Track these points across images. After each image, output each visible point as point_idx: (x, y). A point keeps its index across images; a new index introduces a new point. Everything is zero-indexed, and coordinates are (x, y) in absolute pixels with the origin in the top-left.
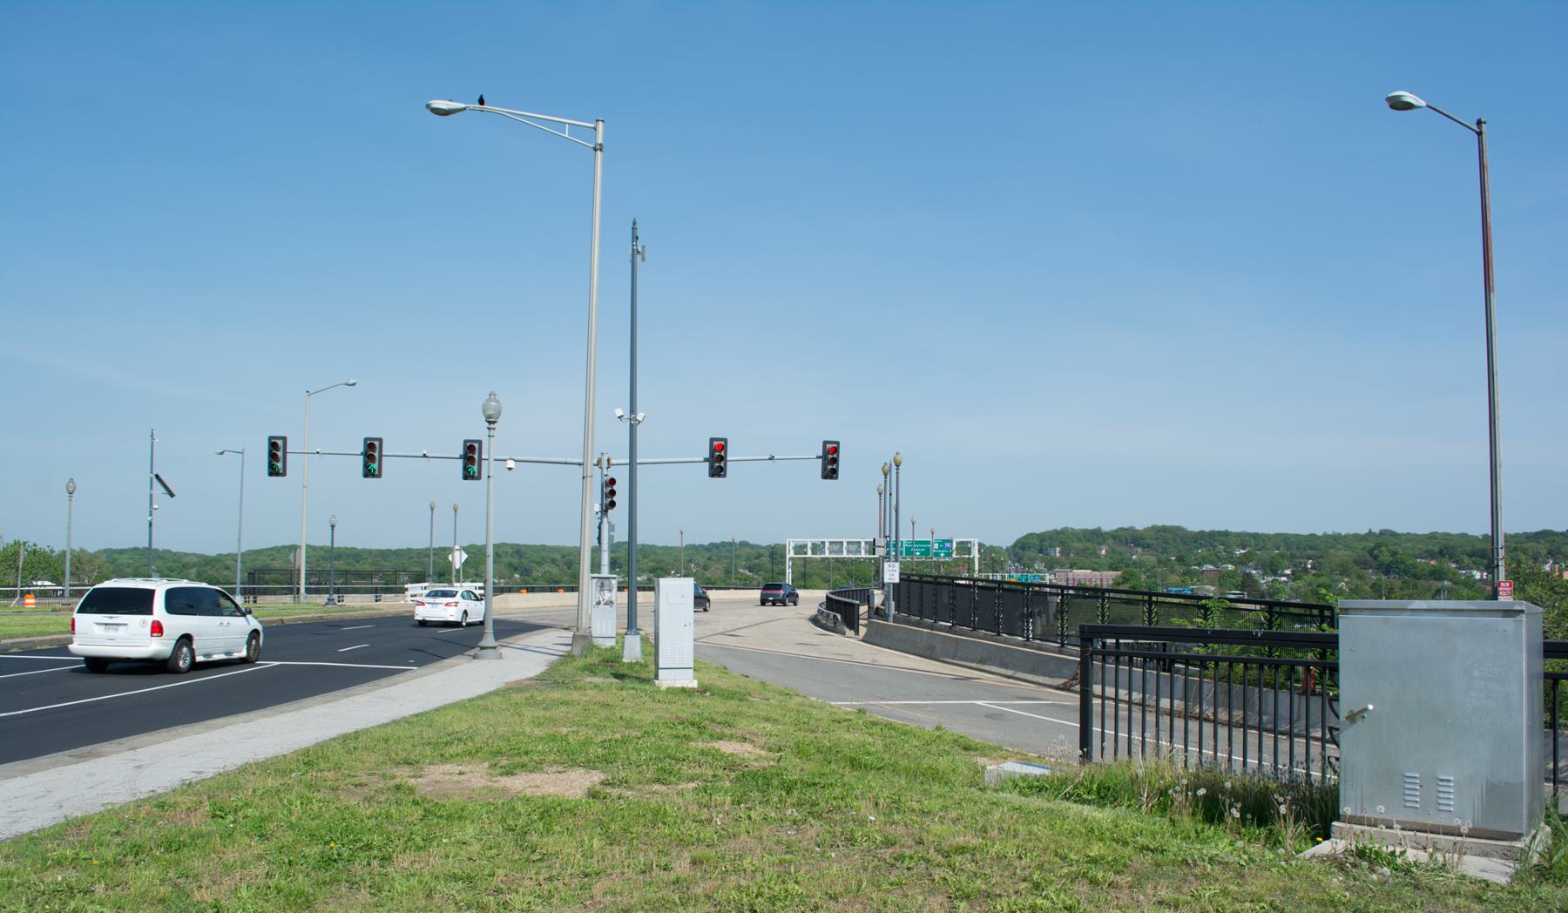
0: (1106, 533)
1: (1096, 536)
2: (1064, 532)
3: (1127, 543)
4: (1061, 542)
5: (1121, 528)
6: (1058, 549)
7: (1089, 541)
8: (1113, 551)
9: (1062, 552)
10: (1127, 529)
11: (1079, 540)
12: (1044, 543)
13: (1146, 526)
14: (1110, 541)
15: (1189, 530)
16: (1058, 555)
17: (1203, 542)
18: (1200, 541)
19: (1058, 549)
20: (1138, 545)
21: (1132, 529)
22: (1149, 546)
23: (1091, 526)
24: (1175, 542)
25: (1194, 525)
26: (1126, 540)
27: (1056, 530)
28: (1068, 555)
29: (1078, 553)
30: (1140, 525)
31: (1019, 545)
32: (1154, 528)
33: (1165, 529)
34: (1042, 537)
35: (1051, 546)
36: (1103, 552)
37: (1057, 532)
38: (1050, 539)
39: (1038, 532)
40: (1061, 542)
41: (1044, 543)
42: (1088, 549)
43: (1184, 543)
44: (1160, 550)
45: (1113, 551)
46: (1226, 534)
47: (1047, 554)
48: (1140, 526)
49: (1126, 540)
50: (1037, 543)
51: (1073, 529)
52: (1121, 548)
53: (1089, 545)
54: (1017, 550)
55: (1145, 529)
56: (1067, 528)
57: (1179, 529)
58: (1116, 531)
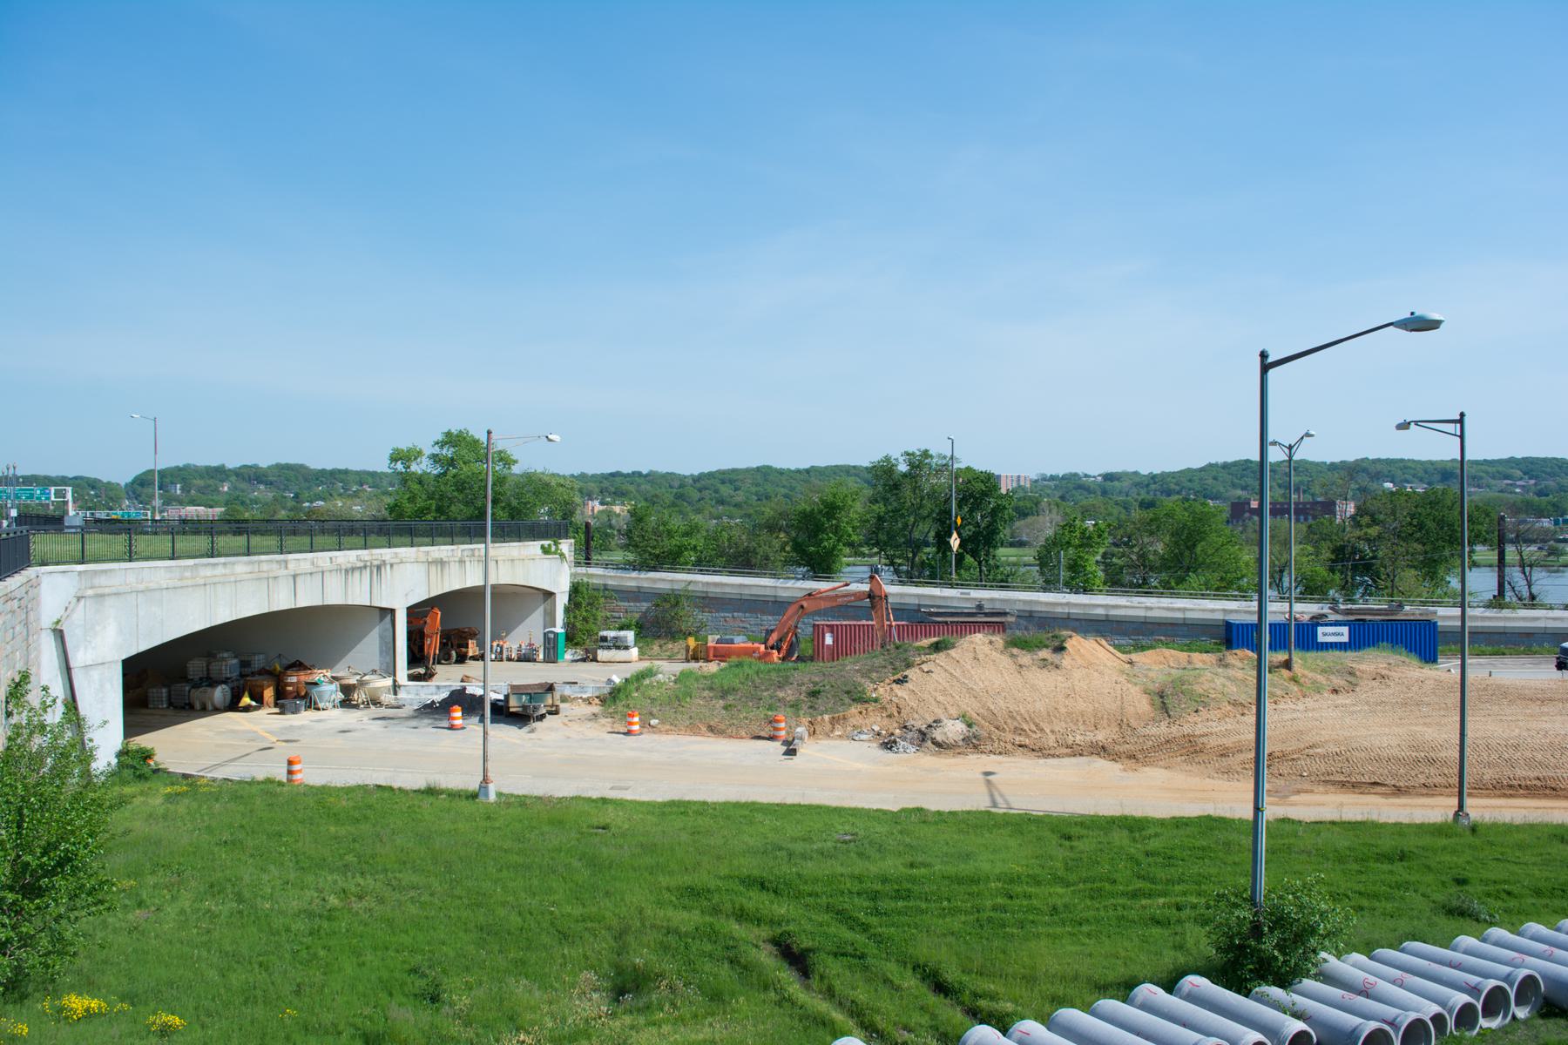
0: (230, 470)
1: (219, 473)
2: (186, 468)
3: (250, 480)
4: (183, 479)
6: (178, 486)
7: (212, 477)
8: (235, 488)
9: (182, 489)
10: (251, 467)
11: (202, 477)
12: (165, 480)
13: (270, 464)
14: (233, 478)
15: (312, 467)
16: (178, 492)
19: (178, 486)
20: (260, 482)
21: (255, 467)
22: (271, 483)
23: (214, 464)
26: (250, 477)
27: (177, 467)
28: (189, 491)
29: (201, 490)
33: (289, 467)
35: (172, 483)
36: (226, 489)
37: (178, 469)
38: (172, 476)
40: (183, 479)
41: (165, 480)
42: (209, 486)
43: (306, 480)
44: (282, 487)
45: (235, 488)
46: (346, 472)
47: (166, 491)
48: (264, 464)
49: (250, 477)
51: (195, 466)
52: (244, 485)
53: (210, 482)
54: (136, 486)
55: (269, 467)
57: (302, 466)
58: (240, 468)
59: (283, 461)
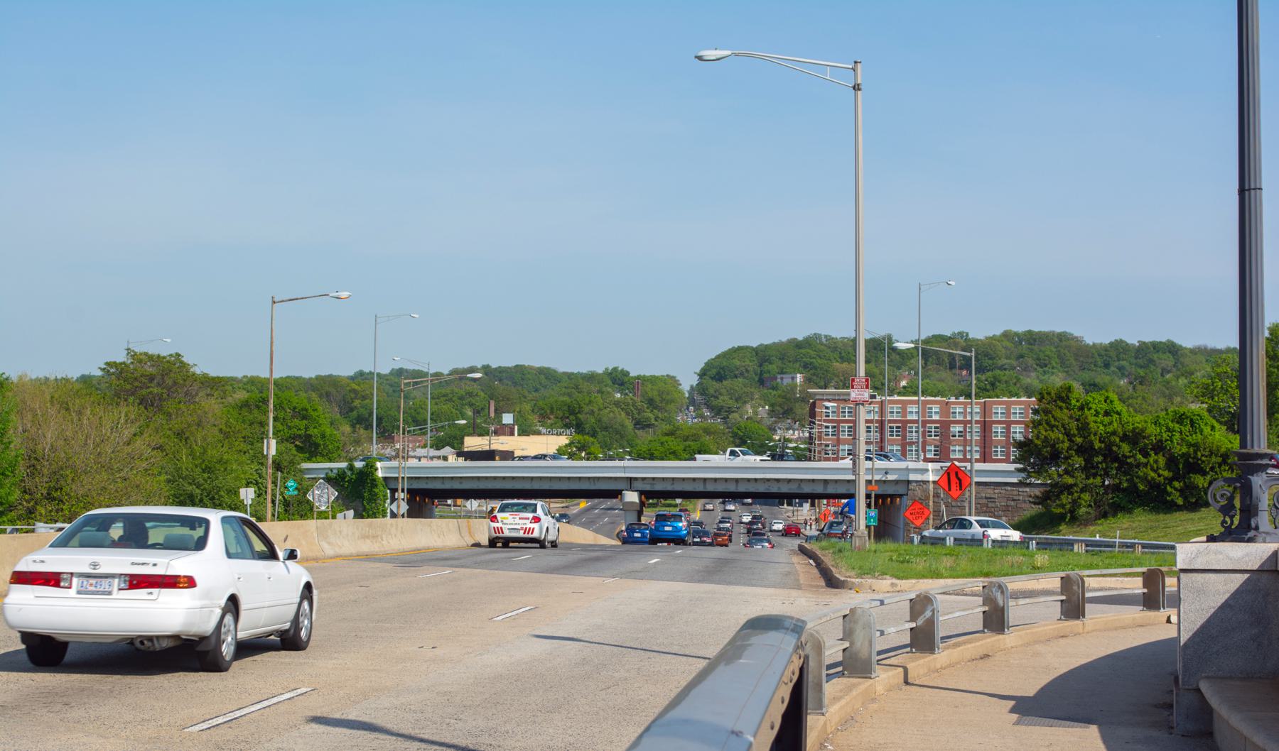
2: (808, 343)
5: (934, 336)
12: (767, 367)
17: (1124, 363)
18: (1117, 364)
24: (1063, 363)
25: (1095, 334)
30: (981, 329)
31: (714, 371)
32: (1007, 335)
34: (762, 355)
35: (782, 373)
37: (796, 345)
38: (782, 359)
39: (755, 346)
46: (1172, 349)
48: (979, 332)
50: (752, 365)
56: (817, 336)
57: (1063, 337)
59: (1020, 327)
